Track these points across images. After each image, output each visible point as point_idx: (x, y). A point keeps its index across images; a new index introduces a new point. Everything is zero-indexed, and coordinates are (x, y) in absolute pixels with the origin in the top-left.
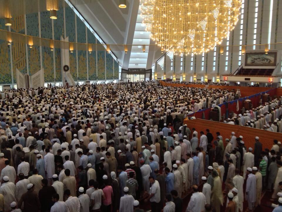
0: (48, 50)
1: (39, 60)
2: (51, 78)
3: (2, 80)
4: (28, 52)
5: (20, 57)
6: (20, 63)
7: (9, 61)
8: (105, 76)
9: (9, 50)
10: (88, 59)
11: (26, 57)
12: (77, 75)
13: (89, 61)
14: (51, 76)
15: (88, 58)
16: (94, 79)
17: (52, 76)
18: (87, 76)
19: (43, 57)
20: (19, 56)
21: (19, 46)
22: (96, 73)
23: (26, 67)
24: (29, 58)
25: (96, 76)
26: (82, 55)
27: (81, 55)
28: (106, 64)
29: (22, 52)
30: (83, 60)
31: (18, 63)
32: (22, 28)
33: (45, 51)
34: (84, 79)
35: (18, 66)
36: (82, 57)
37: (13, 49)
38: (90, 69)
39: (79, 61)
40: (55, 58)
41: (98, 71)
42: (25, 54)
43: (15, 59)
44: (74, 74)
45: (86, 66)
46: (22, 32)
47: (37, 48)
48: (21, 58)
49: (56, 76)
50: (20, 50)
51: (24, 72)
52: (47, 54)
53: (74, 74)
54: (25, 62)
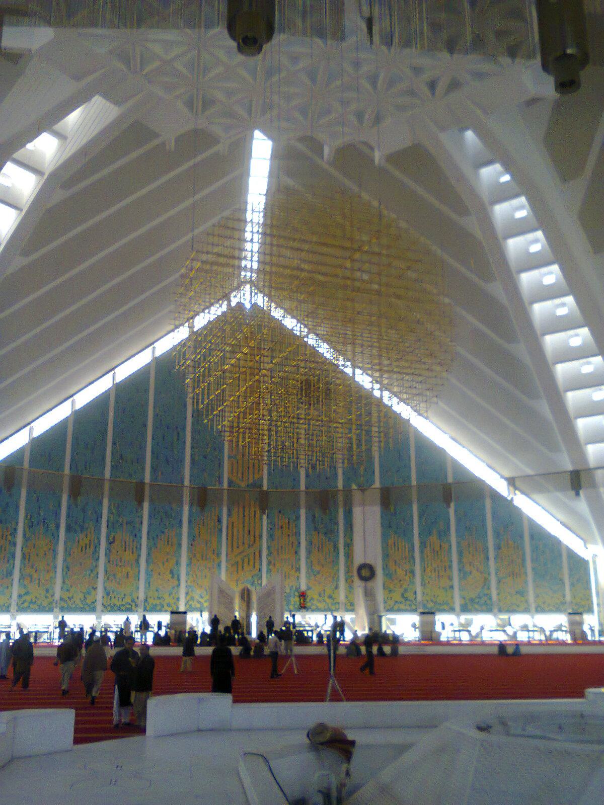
0: (322, 526)
1: (296, 553)
2: (329, 601)
3: (195, 601)
4: (268, 532)
5: (246, 546)
6: (246, 560)
7: (219, 555)
8: (527, 601)
9: (221, 530)
10: (458, 547)
11: (261, 546)
12: (415, 593)
13: (460, 553)
14: (330, 597)
15: (458, 543)
16: (484, 608)
17: (333, 596)
18: (452, 597)
19: (310, 543)
20: (243, 543)
21: (247, 519)
22: (489, 589)
23: (260, 570)
24: (269, 548)
25: (490, 599)
26: (435, 532)
27: (430, 533)
28: (532, 561)
29: (246, 531)
30: (438, 549)
31: (240, 560)
32: (257, 476)
33: (316, 529)
34: (442, 607)
35: (240, 568)
36: (434, 538)
37: (230, 526)
38: (464, 576)
39: (422, 552)
40: (345, 546)
41: (499, 582)
42: (261, 537)
43: (232, 551)
44: (406, 590)
45: (450, 567)
46: (255, 483)
47: (291, 521)
48: (249, 546)
49: (347, 597)
50: (246, 529)
51: (253, 582)
52: (322, 536)
53: (406, 590)
54: (257, 557)
